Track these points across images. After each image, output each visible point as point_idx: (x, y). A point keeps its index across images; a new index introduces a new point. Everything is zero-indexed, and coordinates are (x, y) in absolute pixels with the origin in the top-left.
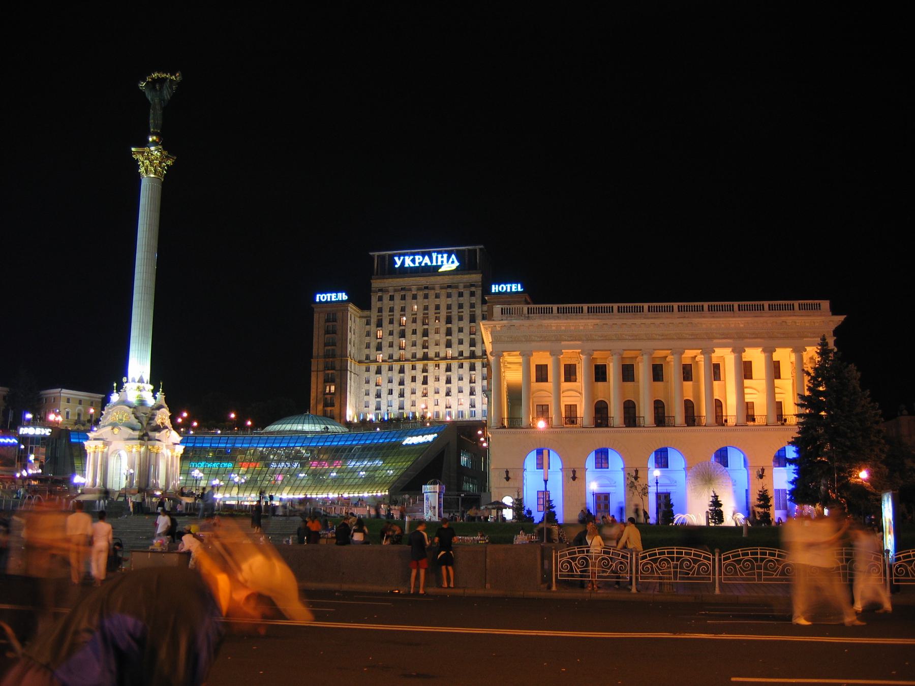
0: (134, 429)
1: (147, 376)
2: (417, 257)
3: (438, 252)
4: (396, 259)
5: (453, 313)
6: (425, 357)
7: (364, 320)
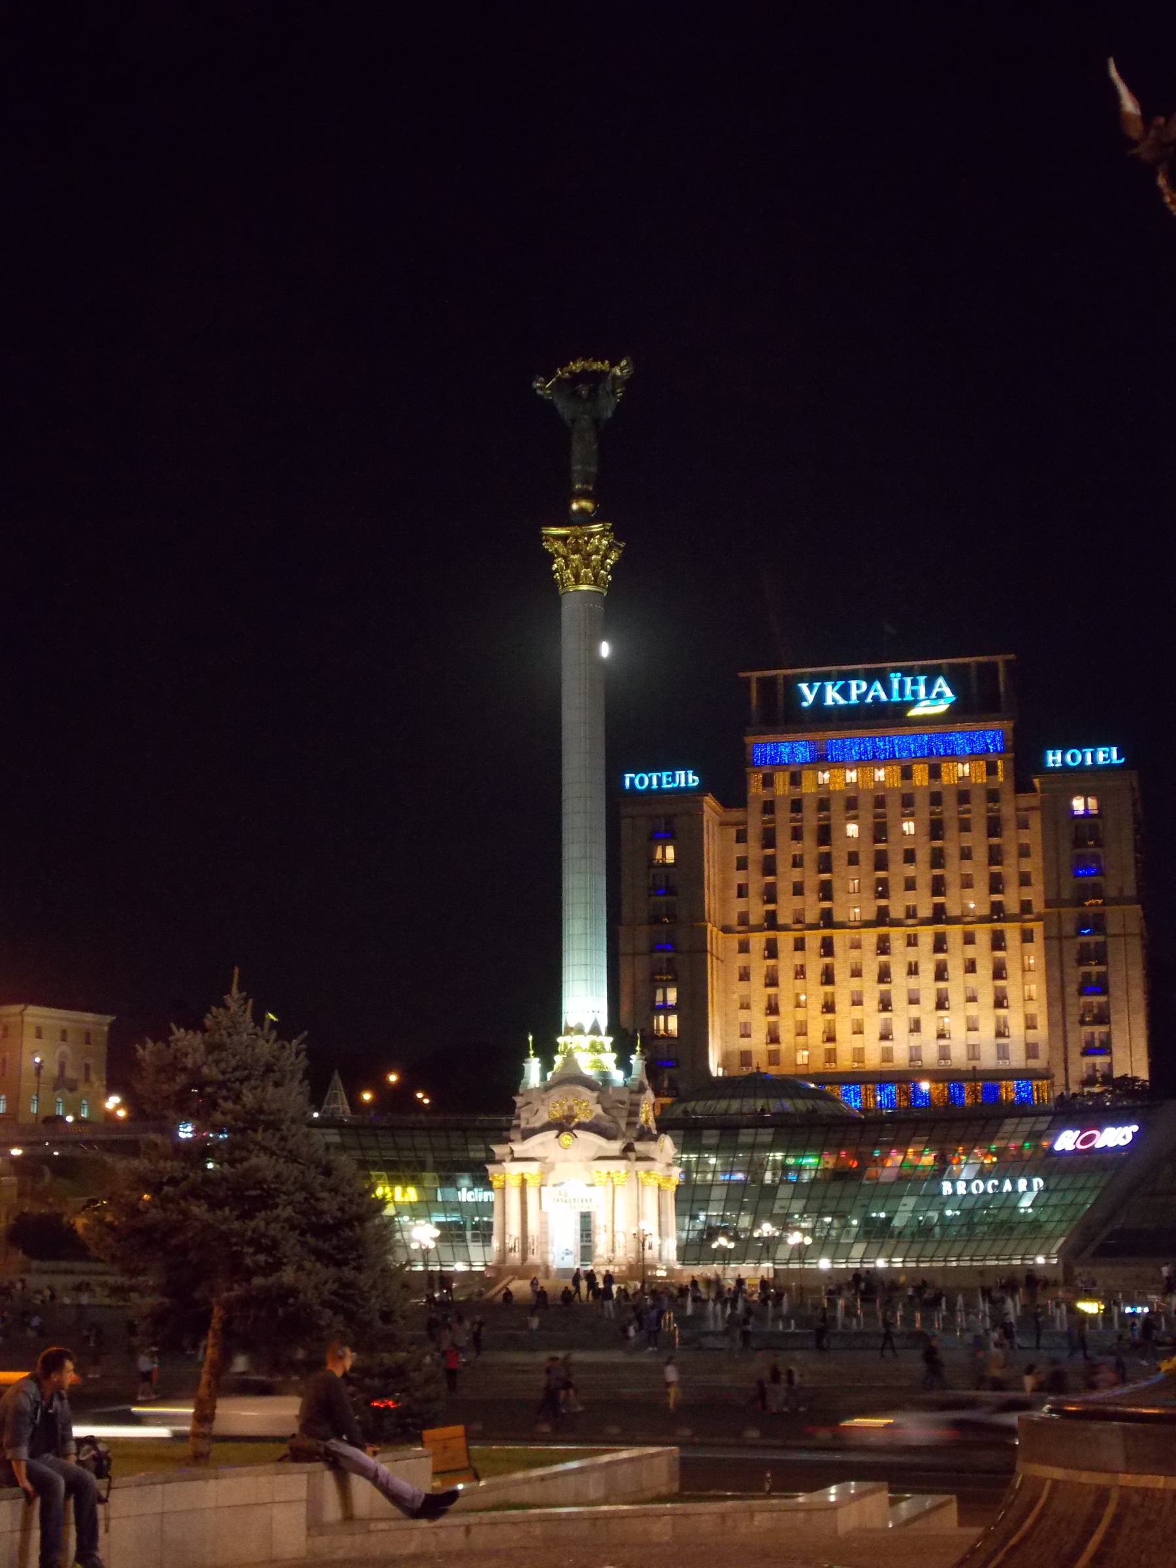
0: (609, 1135)
1: (604, 1024)
2: (853, 683)
3: (906, 672)
4: (804, 687)
5: (946, 814)
6: (882, 918)
7: (732, 832)
